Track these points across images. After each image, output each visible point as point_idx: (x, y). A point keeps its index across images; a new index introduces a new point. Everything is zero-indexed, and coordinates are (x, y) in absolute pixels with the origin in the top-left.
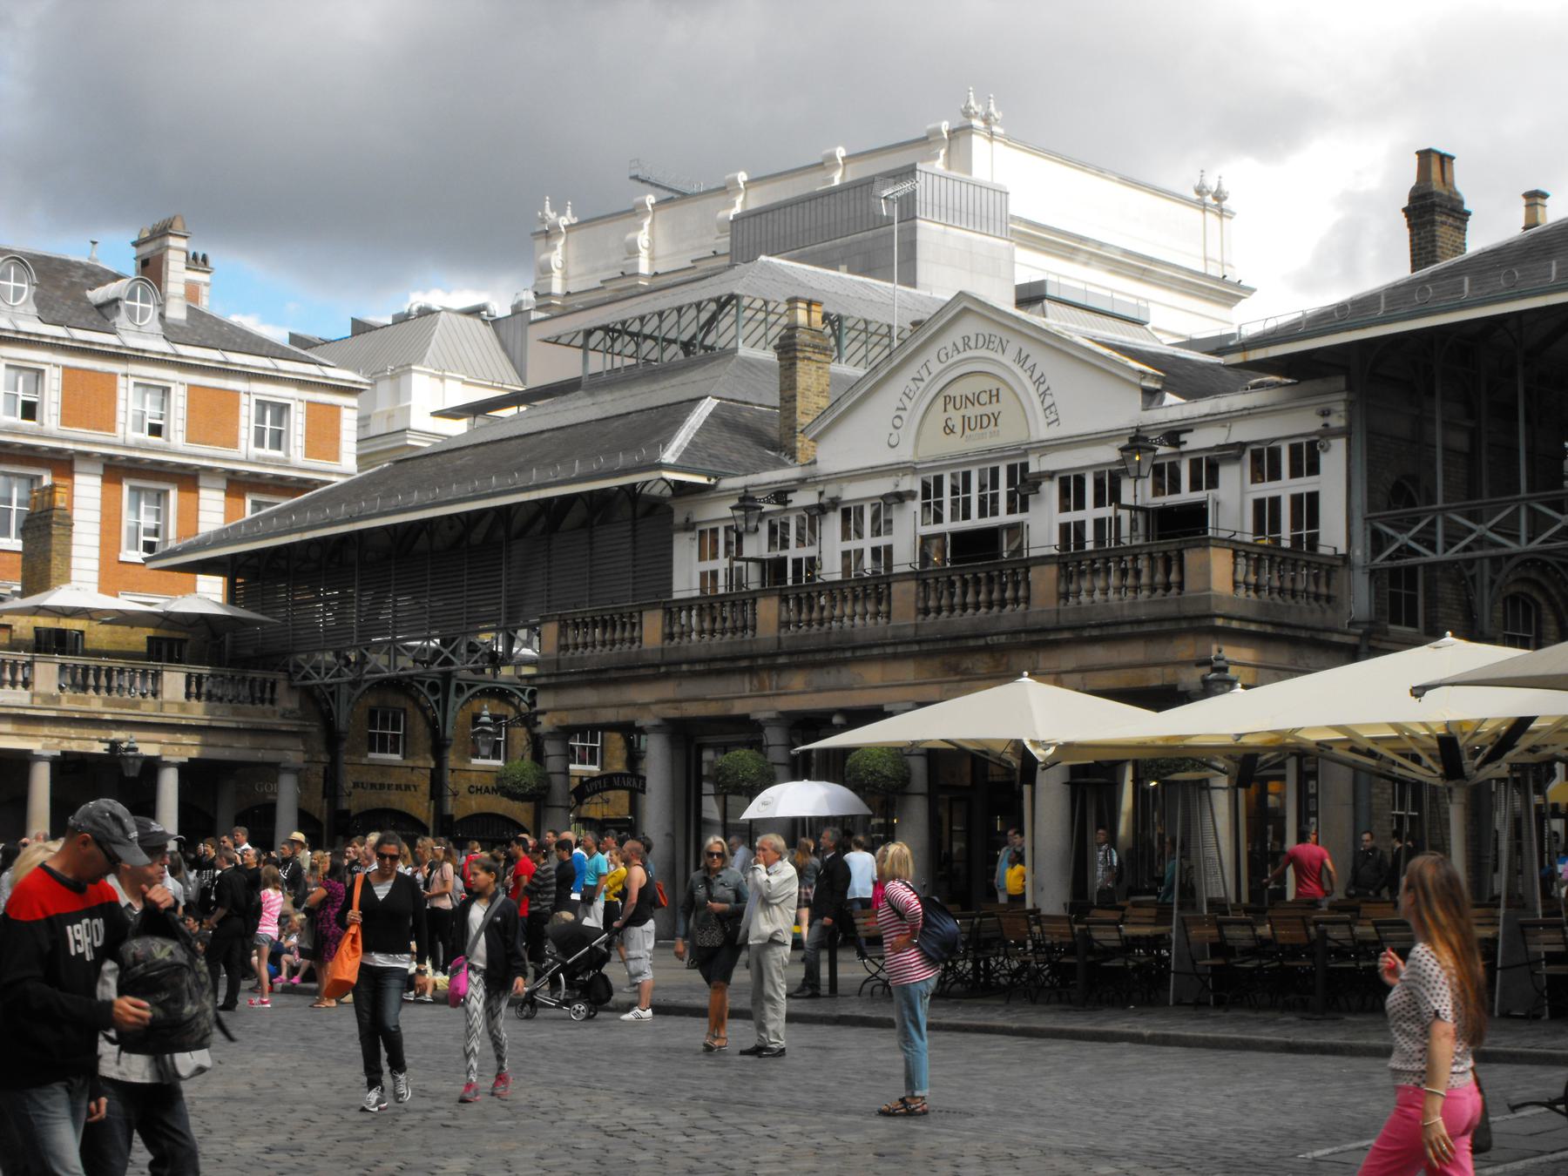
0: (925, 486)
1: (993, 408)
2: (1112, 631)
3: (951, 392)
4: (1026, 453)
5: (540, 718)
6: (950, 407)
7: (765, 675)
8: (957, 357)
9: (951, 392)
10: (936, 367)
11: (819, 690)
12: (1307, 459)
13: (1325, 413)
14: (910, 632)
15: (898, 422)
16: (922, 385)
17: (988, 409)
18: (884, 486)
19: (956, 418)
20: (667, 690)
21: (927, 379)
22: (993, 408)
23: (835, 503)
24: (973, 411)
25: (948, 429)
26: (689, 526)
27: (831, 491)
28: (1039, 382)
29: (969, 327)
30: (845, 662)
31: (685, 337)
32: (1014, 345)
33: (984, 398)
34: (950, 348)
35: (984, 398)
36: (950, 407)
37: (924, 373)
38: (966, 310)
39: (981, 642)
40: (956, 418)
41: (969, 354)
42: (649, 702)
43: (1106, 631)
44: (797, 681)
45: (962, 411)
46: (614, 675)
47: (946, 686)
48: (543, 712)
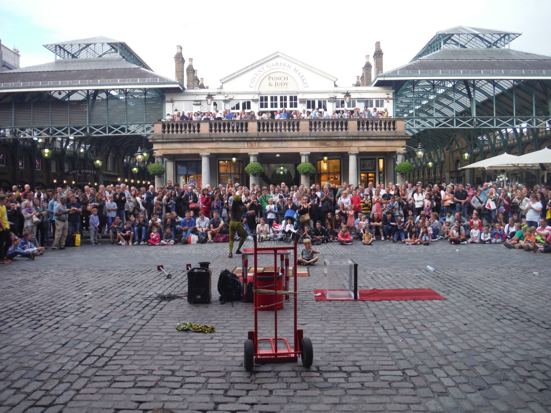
0: (262, 99)
1: (286, 81)
2: (380, 138)
4: (298, 93)
7: (253, 143)
8: (273, 67)
9: (270, 75)
10: (266, 69)
11: (275, 148)
12: (380, 103)
14: (308, 134)
15: (253, 81)
16: (262, 73)
17: (284, 81)
19: (273, 83)
20: (213, 145)
21: (263, 72)
22: (286, 81)
24: (279, 82)
25: (270, 85)
28: (302, 77)
29: (278, 60)
30: (285, 141)
31: (73, 53)
32: (293, 66)
33: (283, 78)
34: (271, 65)
35: (283, 78)
36: (271, 79)
37: (262, 70)
38: (278, 56)
39: (337, 138)
40: (273, 83)
41: (277, 67)
42: (354, 148)
43: (378, 138)
44: (266, 145)
45: (275, 81)
46: (193, 140)
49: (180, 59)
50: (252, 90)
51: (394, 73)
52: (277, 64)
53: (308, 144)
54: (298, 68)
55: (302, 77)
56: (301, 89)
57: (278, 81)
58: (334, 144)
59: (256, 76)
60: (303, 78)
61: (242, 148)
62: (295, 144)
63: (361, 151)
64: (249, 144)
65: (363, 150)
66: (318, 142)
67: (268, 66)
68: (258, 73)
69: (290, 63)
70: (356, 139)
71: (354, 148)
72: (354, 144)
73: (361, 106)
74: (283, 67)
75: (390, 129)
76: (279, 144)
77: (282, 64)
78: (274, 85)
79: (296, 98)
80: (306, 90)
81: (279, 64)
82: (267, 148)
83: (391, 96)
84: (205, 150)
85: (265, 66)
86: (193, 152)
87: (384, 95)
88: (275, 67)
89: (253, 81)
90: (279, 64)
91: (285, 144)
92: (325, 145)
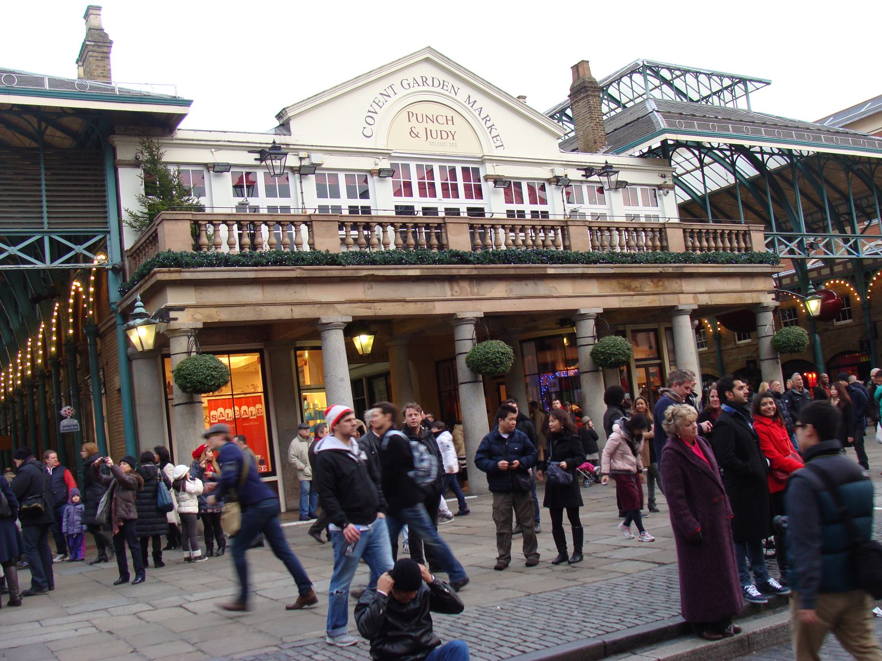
1: (449, 128)
3: (414, 109)
5: (173, 314)
6: (413, 119)
8: (417, 89)
13: (663, 176)
15: (370, 120)
18: (368, 164)
22: (449, 128)
23: (314, 168)
27: (316, 158)
32: (464, 92)
33: (442, 120)
34: (411, 82)
35: (442, 120)
36: (413, 119)
40: (420, 129)
41: (426, 88)
45: (424, 125)
47: (622, 298)
48: (181, 309)
52: (425, 81)
53: (593, 287)
54: (475, 95)
55: (486, 119)
56: (490, 150)
57: (430, 126)
59: (377, 108)
60: (489, 124)
61: (438, 300)
63: (700, 303)
64: (456, 288)
65: (704, 300)
67: (405, 83)
68: (380, 97)
69: (457, 84)
72: (688, 286)
74: (439, 90)
77: (436, 83)
78: (422, 134)
79: (476, 171)
81: (430, 82)
85: (395, 80)
86: (299, 313)
88: (422, 88)
89: (370, 120)
90: (430, 82)
92: (629, 288)
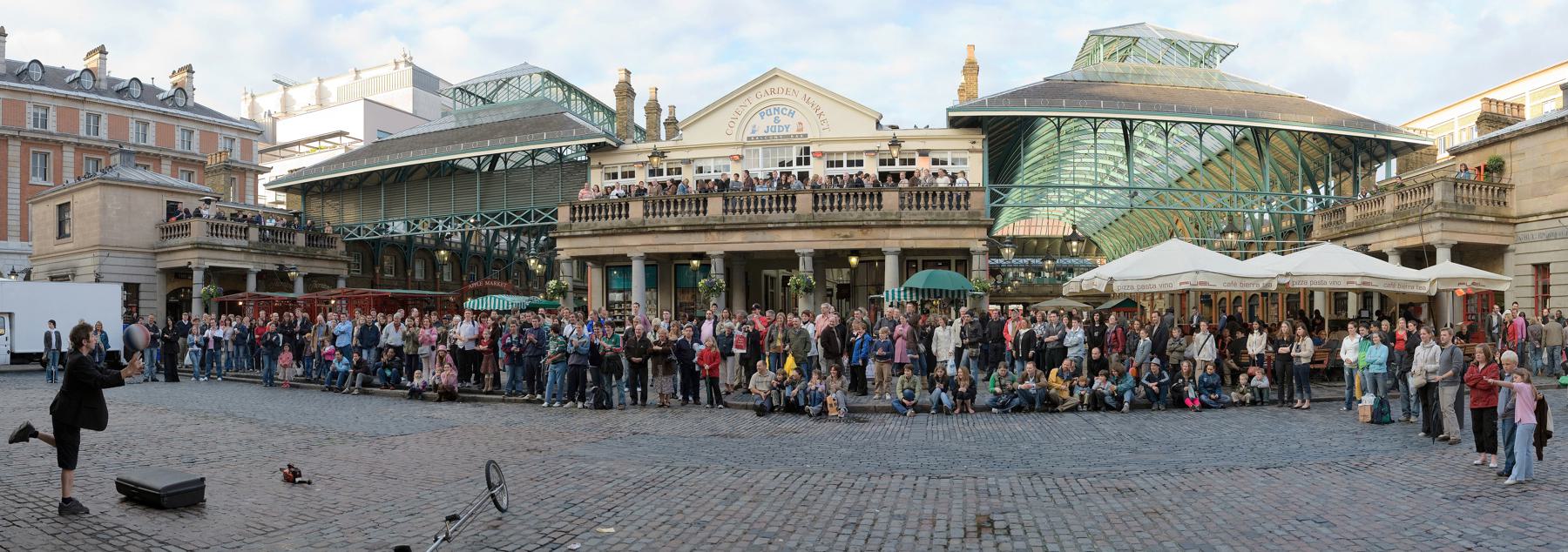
20: (649, 239)
26: (601, 166)
49: (625, 92)
50: (732, 139)
51: (996, 101)
53: (808, 235)
58: (857, 233)
61: (696, 243)
62: (786, 236)
66: (828, 231)
70: (896, 225)
71: (892, 242)
72: (892, 233)
73: (922, 166)
75: (918, 207)
76: (759, 236)
79: (807, 150)
80: (827, 135)
82: (738, 242)
83: (978, 146)
84: (635, 247)
85: (752, 95)
86: (617, 251)
87: (967, 145)
91: (770, 235)
